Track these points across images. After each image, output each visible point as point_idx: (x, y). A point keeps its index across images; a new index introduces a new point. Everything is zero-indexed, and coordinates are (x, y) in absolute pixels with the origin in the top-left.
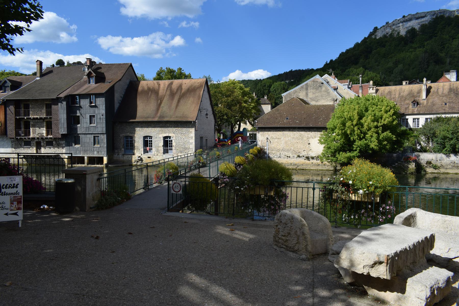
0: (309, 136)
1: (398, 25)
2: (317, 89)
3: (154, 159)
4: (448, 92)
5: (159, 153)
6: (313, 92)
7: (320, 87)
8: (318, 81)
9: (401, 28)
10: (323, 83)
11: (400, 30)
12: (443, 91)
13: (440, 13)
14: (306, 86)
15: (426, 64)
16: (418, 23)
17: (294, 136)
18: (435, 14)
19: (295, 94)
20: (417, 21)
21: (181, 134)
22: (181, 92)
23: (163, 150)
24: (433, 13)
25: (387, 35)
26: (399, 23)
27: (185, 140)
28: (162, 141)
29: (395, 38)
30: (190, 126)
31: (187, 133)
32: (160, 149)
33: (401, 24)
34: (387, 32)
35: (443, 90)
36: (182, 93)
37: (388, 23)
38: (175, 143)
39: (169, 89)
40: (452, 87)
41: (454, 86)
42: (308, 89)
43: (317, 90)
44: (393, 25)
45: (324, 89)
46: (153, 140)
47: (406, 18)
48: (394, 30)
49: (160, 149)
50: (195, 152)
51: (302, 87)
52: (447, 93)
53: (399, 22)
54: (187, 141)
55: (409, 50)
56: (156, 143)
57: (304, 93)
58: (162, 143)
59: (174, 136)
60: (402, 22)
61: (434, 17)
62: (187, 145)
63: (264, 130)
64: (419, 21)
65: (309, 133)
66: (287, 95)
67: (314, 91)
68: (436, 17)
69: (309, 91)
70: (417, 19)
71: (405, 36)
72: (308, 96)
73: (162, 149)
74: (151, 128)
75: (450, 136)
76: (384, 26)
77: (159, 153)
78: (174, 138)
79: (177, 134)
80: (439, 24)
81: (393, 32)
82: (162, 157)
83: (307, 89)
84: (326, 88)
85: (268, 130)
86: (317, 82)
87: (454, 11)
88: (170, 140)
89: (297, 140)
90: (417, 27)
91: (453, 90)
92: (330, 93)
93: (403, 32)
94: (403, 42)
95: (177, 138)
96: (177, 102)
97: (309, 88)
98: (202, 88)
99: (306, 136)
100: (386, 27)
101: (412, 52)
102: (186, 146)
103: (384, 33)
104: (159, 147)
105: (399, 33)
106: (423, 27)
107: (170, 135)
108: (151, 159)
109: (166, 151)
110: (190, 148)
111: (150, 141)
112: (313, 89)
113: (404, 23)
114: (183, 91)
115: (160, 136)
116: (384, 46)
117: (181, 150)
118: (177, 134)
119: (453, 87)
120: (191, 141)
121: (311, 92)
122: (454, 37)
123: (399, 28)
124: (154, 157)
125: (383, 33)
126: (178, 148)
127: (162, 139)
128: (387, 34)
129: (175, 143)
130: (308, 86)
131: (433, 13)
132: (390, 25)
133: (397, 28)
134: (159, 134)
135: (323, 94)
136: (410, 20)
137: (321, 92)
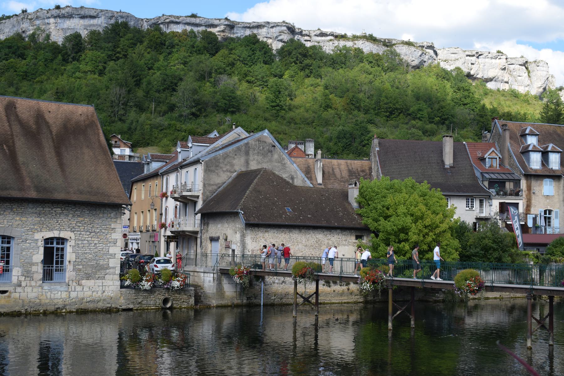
0: (330, 242)
1: (46, 21)
2: (264, 155)
3: (17, 295)
4: (349, 176)
5: (32, 279)
6: (257, 160)
7: (269, 152)
8: (267, 141)
9: (53, 28)
10: (274, 146)
11: (51, 30)
12: (341, 174)
13: (122, 17)
14: (246, 147)
15: (122, 107)
16: (84, 25)
17: (307, 243)
18: (112, 16)
19: (226, 160)
20: (82, 22)
21: (91, 233)
22: (51, 132)
23: (42, 271)
24: (111, 15)
25: (24, 35)
26: (49, 18)
27: (100, 246)
28: (42, 250)
29: (43, 43)
30: (112, 215)
31: (103, 231)
32: (34, 269)
33: (52, 20)
34: (24, 30)
35: (340, 171)
36: (54, 133)
37: (26, 11)
38: (74, 254)
39: (12, 118)
40: (350, 168)
41: (353, 167)
42: (249, 153)
43: (265, 157)
44: (37, 18)
45: (276, 156)
46: (14, 247)
47: (63, 12)
48: (38, 29)
49: (34, 269)
50: (121, 275)
51: (239, 149)
52: (348, 177)
53: (49, 15)
54: (104, 250)
55: (74, 73)
56: (24, 253)
57: (243, 160)
58: (39, 256)
59: (73, 237)
60: (55, 17)
61: (113, 21)
62: (104, 260)
63: (256, 229)
64: (87, 22)
65: (329, 237)
66: (210, 160)
67: (260, 158)
68: (117, 23)
69: (251, 158)
70: (83, 17)
71: (62, 44)
72: (249, 166)
73: (38, 270)
74: (11, 217)
75: (494, 246)
76: (16, 15)
77: (32, 279)
78: (72, 243)
79: (80, 234)
80: (121, 37)
81: (38, 32)
82: (40, 290)
83: (247, 153)
84: (280, 156)
85: (265, 230)
86: (265, 142)
87: (142, 20)
88: (58, 246)
89: (311, 250)
90: (84, 34)
91: (354, 173)
92: (287, 165)
93: (58, 38)
94: (60, 57)
95: (80, 242)
96: (53, 154)
97: (251, 152)
98: (98, 129)
99: (326, 243)
100: (22, 19)
101: (79, 78)
102: (101, 262)
103: (18, 29)
104: (32, 264)
105: (48, 36)
106: (93, 34)
107: (63, 235)
108: (9, 297)
109: (48, 276)
110: (111, 265)
111: (58, 249)
112: (258, 155)
113: (59, 20)
114: (54, 130)
115: (36, 238)
116: (22, 56)
117: (89, 271)
118: (80, 234)
119: (353, 169)
120: (112, 250)
121: (254, 159)
122: (149, 66)
123: (48, 27)
124: (19, 289)
125: (15, 29)
126: (81, 267)
127: (41, 244)
128: (24, 32)
129: (74, 254)
130: (249, 147)
131: (110, 15)
132: (29, 17)
133: (44, 25)
134: (33, 231)
135: (275, 166)
136: (70, 16)
137: (271, 161)
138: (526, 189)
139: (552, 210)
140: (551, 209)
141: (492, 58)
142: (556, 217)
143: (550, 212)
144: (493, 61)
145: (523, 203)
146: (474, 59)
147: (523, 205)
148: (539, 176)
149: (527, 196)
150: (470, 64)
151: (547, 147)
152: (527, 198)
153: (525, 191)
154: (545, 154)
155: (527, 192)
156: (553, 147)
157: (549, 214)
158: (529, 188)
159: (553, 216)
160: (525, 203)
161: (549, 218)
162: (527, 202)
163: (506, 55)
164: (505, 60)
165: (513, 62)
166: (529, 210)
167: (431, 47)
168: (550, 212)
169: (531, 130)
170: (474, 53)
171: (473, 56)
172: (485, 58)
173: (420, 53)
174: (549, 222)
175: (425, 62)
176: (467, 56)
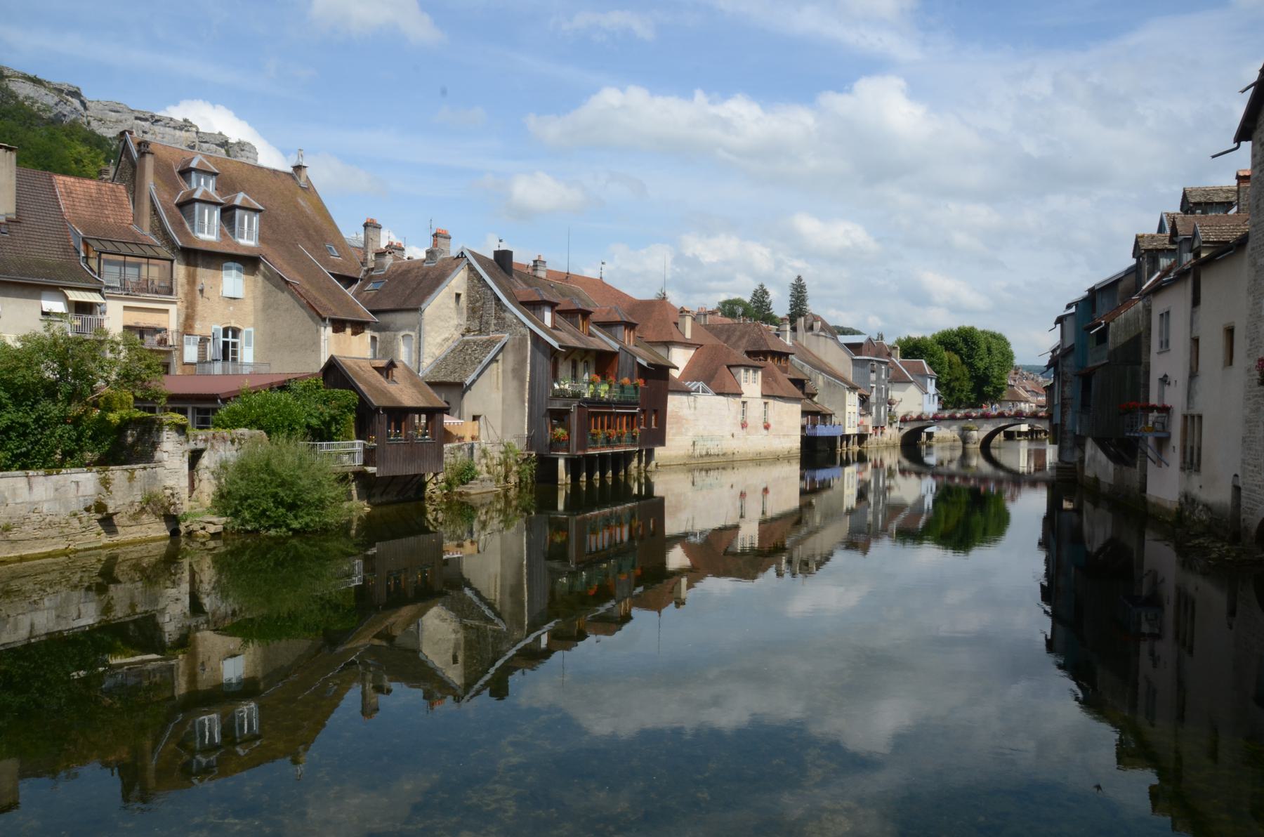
138: (184, 281)
139: (239, 330)
140: (238, 326)
141: (175, 128)
142: (248, 344)
143: (236, 332)
144: (178, 133)
145: (178, 310)
146: (146, 125)
147: (178, 315)
148: (214, 259)
149: (186, 295)
150: (140, 132)
151: (234, 198)
152: (187, 301)
153: (182, 286)
154: (228, 213)
155: (186, 287)
156: (244, 199)
157: (234, 336)
158: (192, 280)
159: (241, 341)
160: (183, 311)
161: (234, 345)
162: (187, 308)
163: (196, 126)
164: (194, 135)
165: (207, 139)
166: (191, 327)
167: (76, 94)
168: (236, 332)
169: (201, 162)
170: (147, 116)
171: (146, 120)
172: (165, 126)
173: (56, 99)
174: (235, 353)
175: (65, 116)
176: (137, 118)
